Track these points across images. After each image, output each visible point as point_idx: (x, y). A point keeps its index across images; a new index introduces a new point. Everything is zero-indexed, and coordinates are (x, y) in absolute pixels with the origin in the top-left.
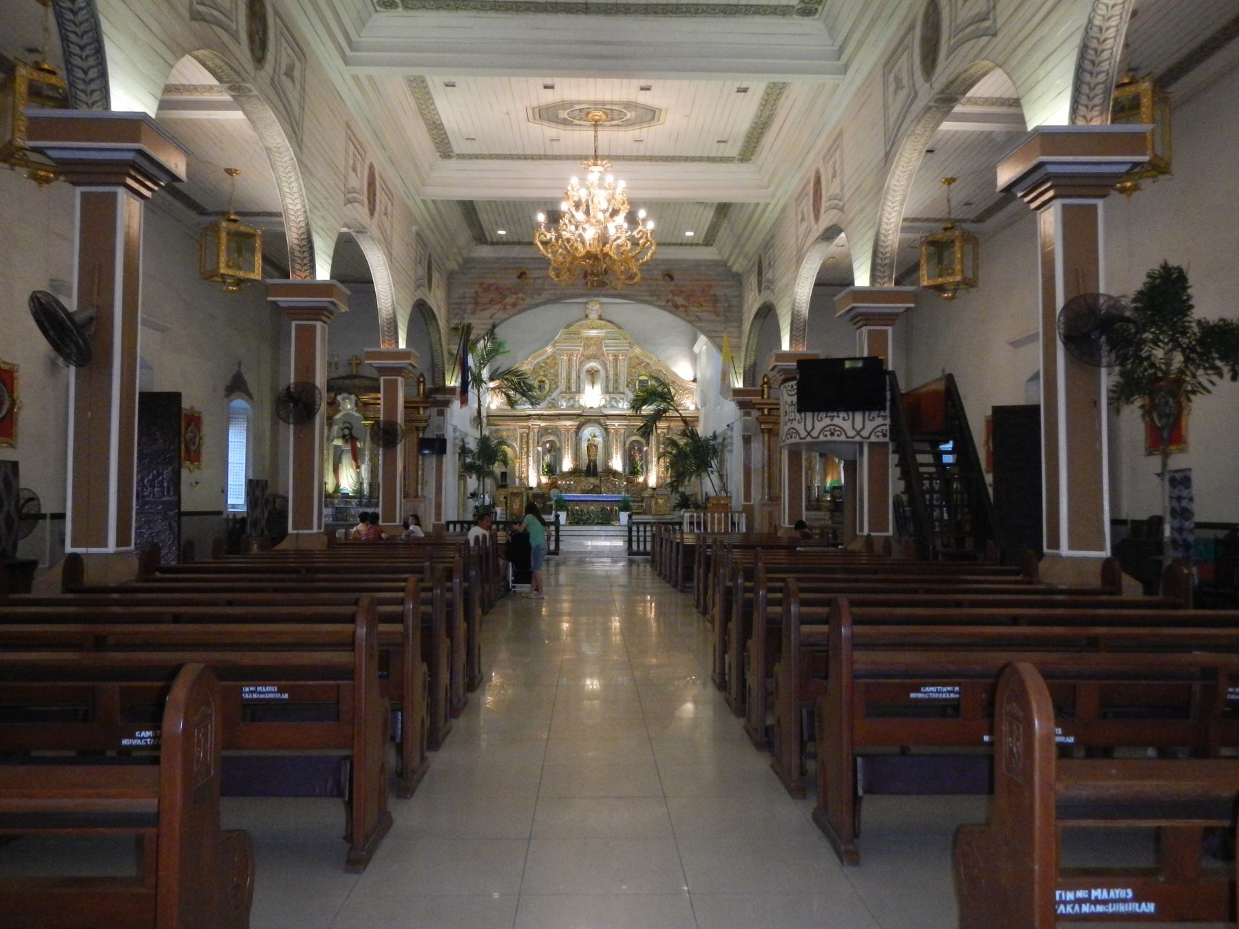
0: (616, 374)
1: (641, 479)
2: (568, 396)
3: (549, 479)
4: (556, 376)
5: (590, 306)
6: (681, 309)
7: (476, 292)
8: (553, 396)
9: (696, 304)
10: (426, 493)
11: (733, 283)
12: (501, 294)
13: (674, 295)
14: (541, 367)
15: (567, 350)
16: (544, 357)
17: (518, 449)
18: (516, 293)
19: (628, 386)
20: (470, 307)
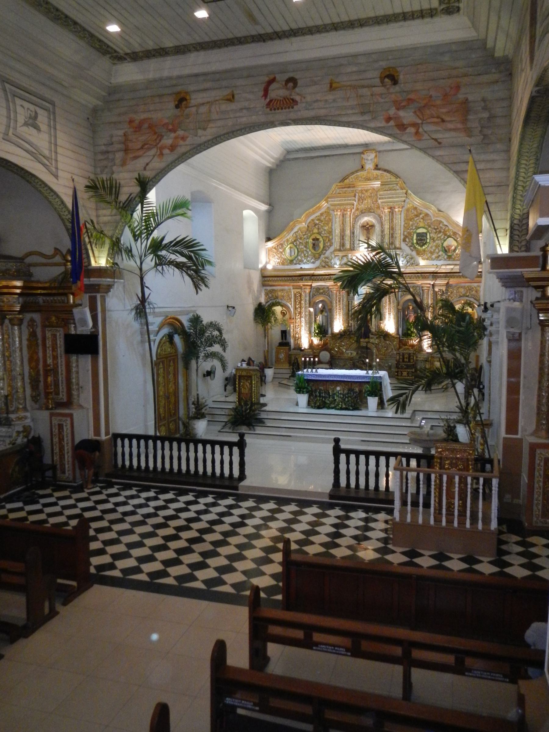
0: (392, 228)
1: (415, 341)
2: (340, 254)
3: (321, 340)
4: (330, 232)
5: (365, 156)
6: (408, 130)
7: (125, 135)
8: (326, 255)
9: (435, 120)
10: (82, 402)
11: (496, 76)
12: (155, 133)
13: (398, 109)
14: (316, 225)
15: (339, 205)
16: (318, 214)
17: (292, 310)
18: (174, 131)
19: (404, 240)
20: (119, 156)
